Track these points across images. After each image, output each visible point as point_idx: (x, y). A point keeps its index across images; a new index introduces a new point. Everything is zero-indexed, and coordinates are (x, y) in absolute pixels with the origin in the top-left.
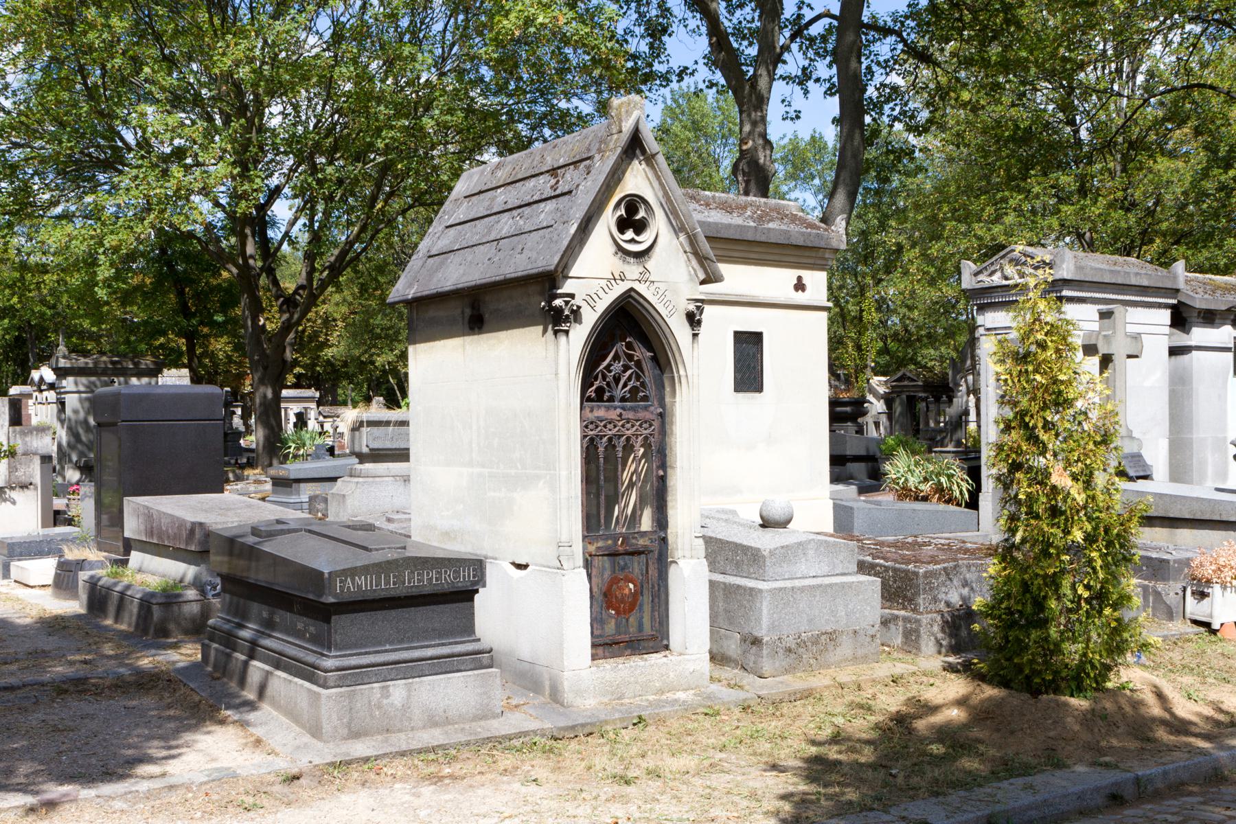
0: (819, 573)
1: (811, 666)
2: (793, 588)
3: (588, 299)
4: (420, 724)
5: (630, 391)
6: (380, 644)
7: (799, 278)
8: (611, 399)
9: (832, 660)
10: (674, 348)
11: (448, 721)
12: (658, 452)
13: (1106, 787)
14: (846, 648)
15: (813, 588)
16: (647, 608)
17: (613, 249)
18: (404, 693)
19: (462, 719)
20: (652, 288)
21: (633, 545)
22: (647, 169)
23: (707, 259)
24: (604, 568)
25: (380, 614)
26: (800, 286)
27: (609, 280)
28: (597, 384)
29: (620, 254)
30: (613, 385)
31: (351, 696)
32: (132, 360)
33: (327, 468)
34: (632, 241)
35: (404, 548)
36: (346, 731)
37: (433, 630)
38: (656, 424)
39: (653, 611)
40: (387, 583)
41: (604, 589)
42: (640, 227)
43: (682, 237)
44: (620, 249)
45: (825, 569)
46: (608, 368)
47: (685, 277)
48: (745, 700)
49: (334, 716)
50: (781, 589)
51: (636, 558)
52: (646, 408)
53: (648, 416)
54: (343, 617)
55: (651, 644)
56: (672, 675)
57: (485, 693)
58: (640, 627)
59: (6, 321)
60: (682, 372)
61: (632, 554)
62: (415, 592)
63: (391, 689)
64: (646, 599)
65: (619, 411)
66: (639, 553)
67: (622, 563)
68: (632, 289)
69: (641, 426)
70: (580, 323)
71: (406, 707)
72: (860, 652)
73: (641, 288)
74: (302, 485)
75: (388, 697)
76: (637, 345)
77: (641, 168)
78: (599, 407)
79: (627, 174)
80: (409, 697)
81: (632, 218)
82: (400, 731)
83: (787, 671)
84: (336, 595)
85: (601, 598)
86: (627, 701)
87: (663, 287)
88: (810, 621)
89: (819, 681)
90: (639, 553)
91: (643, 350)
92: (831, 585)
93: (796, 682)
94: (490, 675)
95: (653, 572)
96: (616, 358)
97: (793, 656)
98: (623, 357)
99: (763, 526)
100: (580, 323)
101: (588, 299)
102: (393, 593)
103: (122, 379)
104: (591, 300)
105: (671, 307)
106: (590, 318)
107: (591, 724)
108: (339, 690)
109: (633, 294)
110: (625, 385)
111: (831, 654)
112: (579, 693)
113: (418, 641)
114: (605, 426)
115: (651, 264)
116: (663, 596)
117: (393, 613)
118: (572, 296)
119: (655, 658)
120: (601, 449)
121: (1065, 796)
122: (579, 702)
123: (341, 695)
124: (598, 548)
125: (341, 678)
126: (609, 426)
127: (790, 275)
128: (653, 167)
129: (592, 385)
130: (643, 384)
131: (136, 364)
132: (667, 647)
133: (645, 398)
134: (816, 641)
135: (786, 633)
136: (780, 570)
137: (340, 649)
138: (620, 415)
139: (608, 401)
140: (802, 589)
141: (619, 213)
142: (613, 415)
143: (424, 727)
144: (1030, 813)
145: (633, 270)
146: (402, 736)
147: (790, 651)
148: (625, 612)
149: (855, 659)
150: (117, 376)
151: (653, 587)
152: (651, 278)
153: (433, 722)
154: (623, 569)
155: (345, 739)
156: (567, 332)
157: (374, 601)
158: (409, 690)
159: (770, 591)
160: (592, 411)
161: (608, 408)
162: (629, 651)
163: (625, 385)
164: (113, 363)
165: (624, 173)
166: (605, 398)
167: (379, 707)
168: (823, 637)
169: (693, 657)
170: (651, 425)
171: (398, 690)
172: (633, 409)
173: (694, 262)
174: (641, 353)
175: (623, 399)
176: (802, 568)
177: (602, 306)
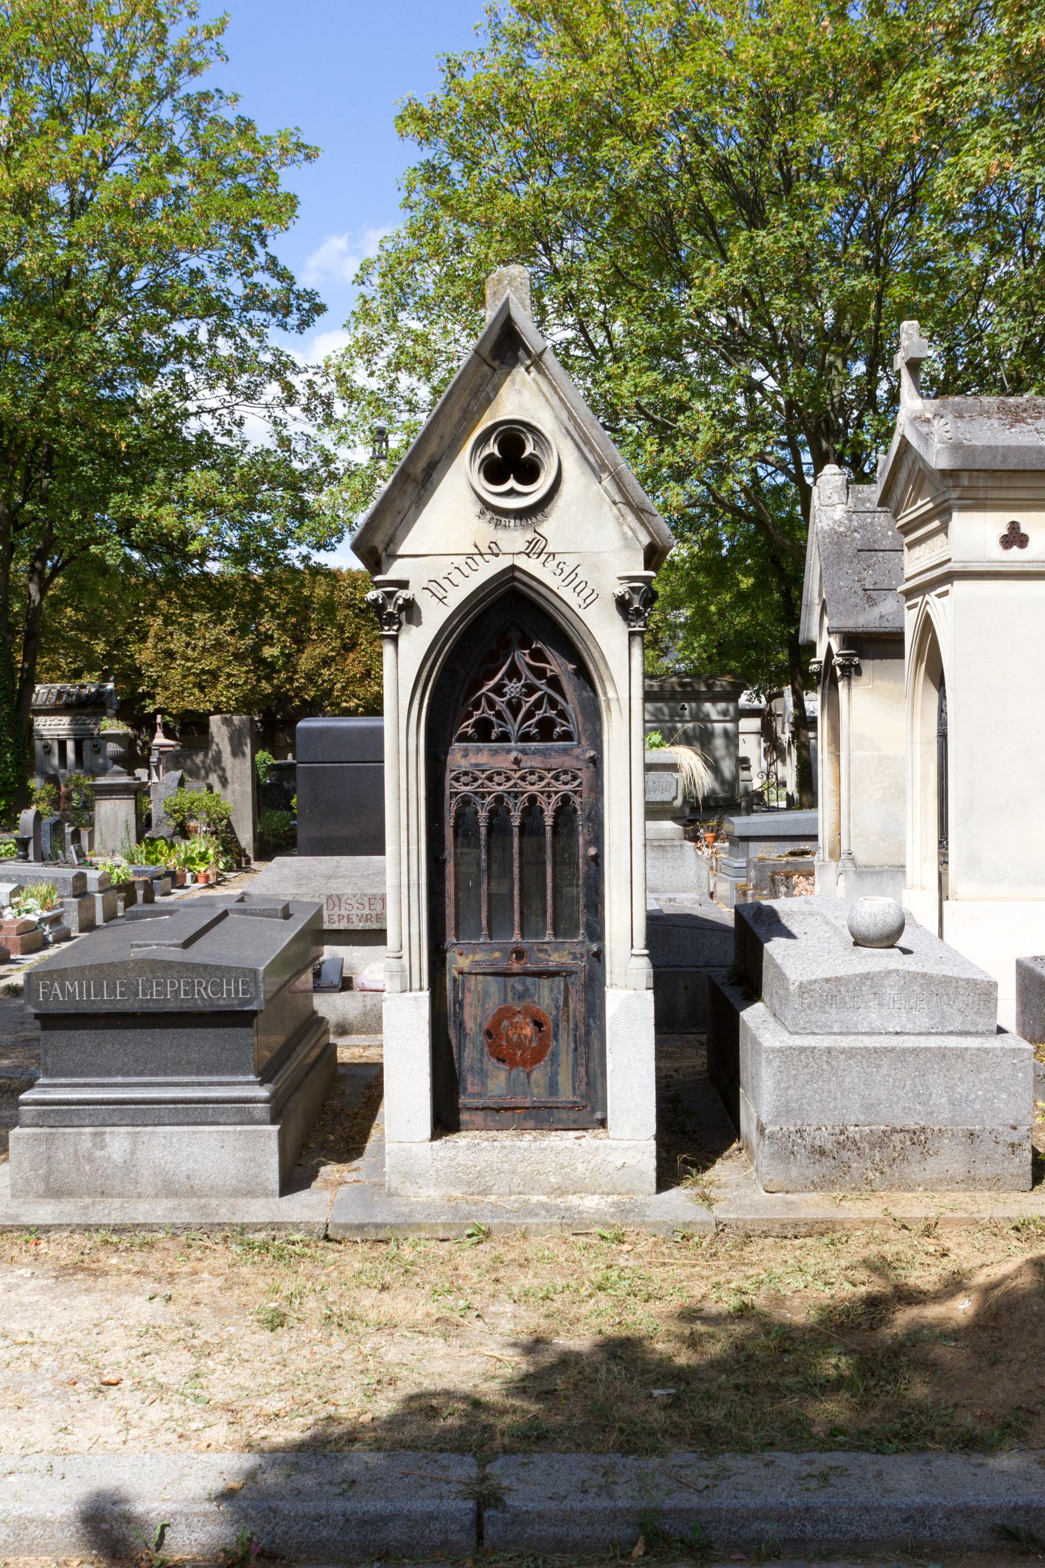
0: (909, 1027)
1: (870, 1182)
2: (829, 1051)
3: (433, 586)
4: (151, 1190)
5: (538, 724)
6: (108, 1074)
7: (1014, 526)
8: (504, 737)
9: (919, 1177)
10: (596, 656)
11: (192, 1192)
12: (589, 818)
13: (994, 1511)
14: (951, 1159)
15: (904, 1053)
16: (566, 1060)
17: (478, 507)
18: (127, 1145)
19: (214, 1191)
20: (552, 564)
21: (541, 960)
22: (540, 379)
23: (643, 510)
24: (486, 994)
25: (109, 1034)
26: (1015, 538)
27: (470, 556)
28: (477, 714)
29: (489, 515)
30: (507, 714)
31: (49, 1140)
32: (705, 682)
33: (797, 822)
34: (511, 493)
35: (889, 939)
36: (42, 1186)
37: (189, 1062)
38: (584, 776)
39: (575, 1065)
40: (112, 991)
41: (486, 1025)
42: (529, 472)
43: (607, 481)
44: (488, 506)
45: (924, 1022)
46: (498, 690)
47: (617, 542)
48: (687, 1224)
49: (26, 1165)
50: (802, 1050)
51: (545, 982)
52: (565, 751)
53: (568, 762)
54: (57, 1033)
55: (573, 1115)
56: (581, 1168)
57: (252, 1159)
58: (553, 1087)
59: (704, 636)
60: (611, 694)
61: (539, 974)
62: (152, 1007)
63: (108, 1138)
64: (565, 1046)
65: (514, 754)
66: (552, 974)
67: (519, 987)
68: (513, 568)
69: (556, 778)
70: (419, 623)
71: (129, 1165)
72: (982, 1171)
73: (531, 565)
74: (752, 844)
75: (103, 1148)
76: (549, 652)
77: (528, 378)
78: (479, 750)
79: (503, 391)
80: (133, 1153)
81: (512, 458)
82: (120, 1195)
83: (815, 1187)
84: (37, 1005)
85: (481, 1037)
86: (492, 1198)
87: (571, 562)
88: (867, 1108)
89: (855, 1209)
90: (552, 974)
91: (562, 661)
92: (915, 1051)
93: (813, 1206)
94: (261, 1135)
95: (577, 1006)
96: (514, 673)
97: (829, 1162)
98: (525, 672)
99: (856, 944)
100: (419, 623)
101: (433, 586)
102: (119, 1008)
103: (694, 705)
104: (436, 589)
105: (588, 591)
106: (435, 615)
107: (392, 1226)
108: (38, 1130)
109: (517, 574)
110: (530, 715)
111: (915, 1167)
112: (408, 1176)
113: (165, 1075)
114: (490, 779)
115: (549, 526)
116: (596, 1045)
117: (129, 1034)
118: (404, 585)
119: (562, 1142)
120: (483, 814)
121: (866, 1509)
122: (409, 1190)
123: (36, 1138)
124: (477, 963)
125: (40, 1114)
126: (463, 779)
127: (997, 522)
128: (540, 371)
129: (470, 716)
130: (562, 714)
131: (710, 687)
132: (603, 1123)
133: (567, 736)
134: (881, 1141)
135: (853, 1120)
136: (823, 1017)
137: (52, 1076)
138: (517, 761)
139: (496, 741)
140: (850, 1053)
141: (486, 452)
142: (504, 762)
143: (157, 1196)
144: (757, 1525)
145: (514, 539)
146: (117, 1202)
147: (822, 1152)
148: (524, 1063)
149: (971, 1182)
150: (688, 700)
151: (576, 1028)
152: (550, 549)
153: (169, 1189)
154: (521, 997)
155: (40, 1196)
156: (395, 639)
157: (145, 1015)
158: (134, 1143)
159: (781, 1050)
160: (466, 756)
161: (495, 752)
162: (531, 1123)
163: (530, 715)
164: (682, 685)
165: (497, 389)
166: (493, 736)
167: (91, 1160)
168: (896, 1138)
169: (624, 1144)
170: (575, 778)
171: (118, 1141)
172: (537, 752)
173: (631, 518)
174: (557, 665)
175: (526, 737)
176: (871, 1016)
177: (456, 597)
